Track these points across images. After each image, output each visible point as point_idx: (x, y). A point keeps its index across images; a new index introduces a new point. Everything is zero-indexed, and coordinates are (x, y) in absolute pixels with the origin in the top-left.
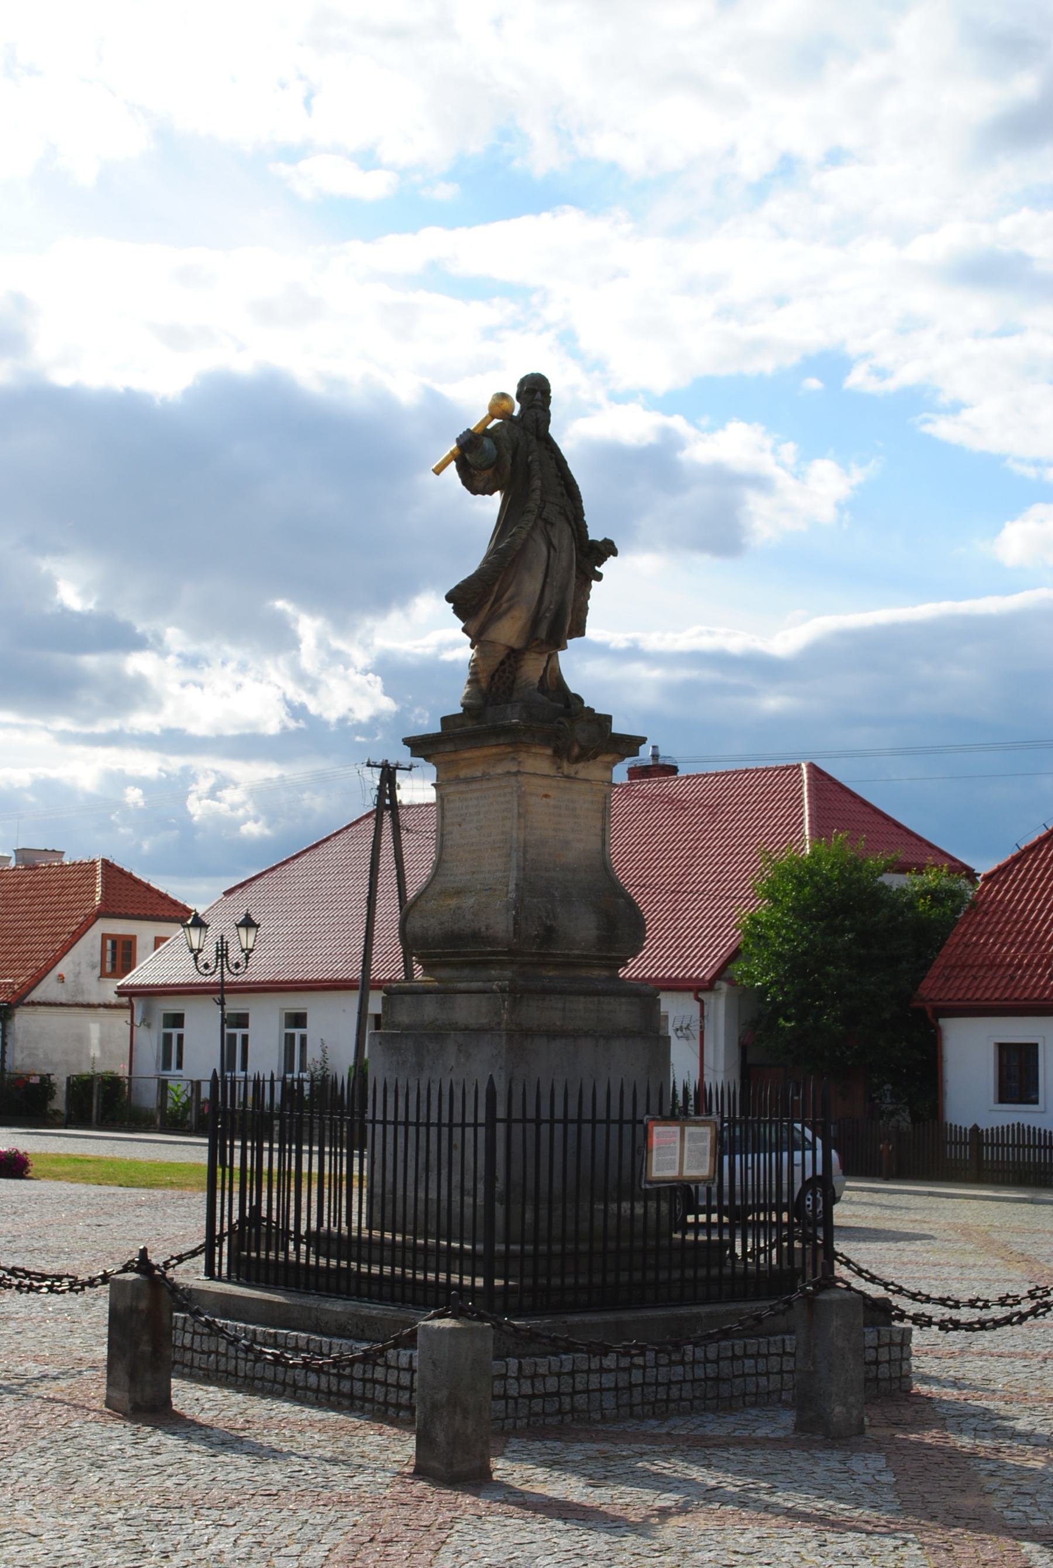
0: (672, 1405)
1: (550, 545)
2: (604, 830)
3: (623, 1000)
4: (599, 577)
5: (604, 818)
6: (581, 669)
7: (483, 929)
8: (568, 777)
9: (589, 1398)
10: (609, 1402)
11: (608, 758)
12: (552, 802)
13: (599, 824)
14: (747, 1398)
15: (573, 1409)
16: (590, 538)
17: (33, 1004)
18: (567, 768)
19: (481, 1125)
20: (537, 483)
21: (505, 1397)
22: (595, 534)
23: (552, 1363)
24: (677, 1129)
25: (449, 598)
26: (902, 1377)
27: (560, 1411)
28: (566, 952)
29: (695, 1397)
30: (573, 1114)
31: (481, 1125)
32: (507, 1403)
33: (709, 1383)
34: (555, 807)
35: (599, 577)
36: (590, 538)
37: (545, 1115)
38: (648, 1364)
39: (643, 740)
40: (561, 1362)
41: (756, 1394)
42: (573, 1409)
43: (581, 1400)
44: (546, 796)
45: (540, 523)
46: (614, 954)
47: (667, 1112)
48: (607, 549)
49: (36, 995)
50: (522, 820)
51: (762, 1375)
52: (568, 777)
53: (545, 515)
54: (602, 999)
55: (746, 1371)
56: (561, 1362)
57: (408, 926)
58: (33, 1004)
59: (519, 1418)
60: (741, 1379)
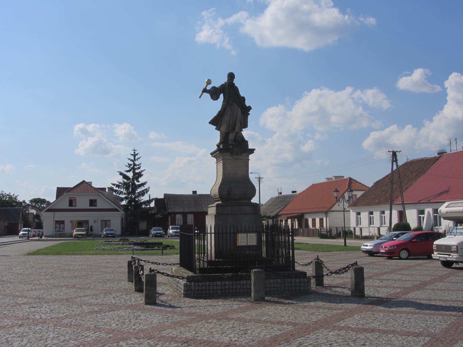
4: (249, 114)
8: (236, 159)
11: (246, 154)
17: (332, 211)
18: (235, 157)
21: (191, 290)
24: (245, 235)
35: (249, 114)
39: (255, 149)
42: (209, 293)
43: (212, 292)
49: (333, 209)
52: (236, 159)
58: (332, 211)
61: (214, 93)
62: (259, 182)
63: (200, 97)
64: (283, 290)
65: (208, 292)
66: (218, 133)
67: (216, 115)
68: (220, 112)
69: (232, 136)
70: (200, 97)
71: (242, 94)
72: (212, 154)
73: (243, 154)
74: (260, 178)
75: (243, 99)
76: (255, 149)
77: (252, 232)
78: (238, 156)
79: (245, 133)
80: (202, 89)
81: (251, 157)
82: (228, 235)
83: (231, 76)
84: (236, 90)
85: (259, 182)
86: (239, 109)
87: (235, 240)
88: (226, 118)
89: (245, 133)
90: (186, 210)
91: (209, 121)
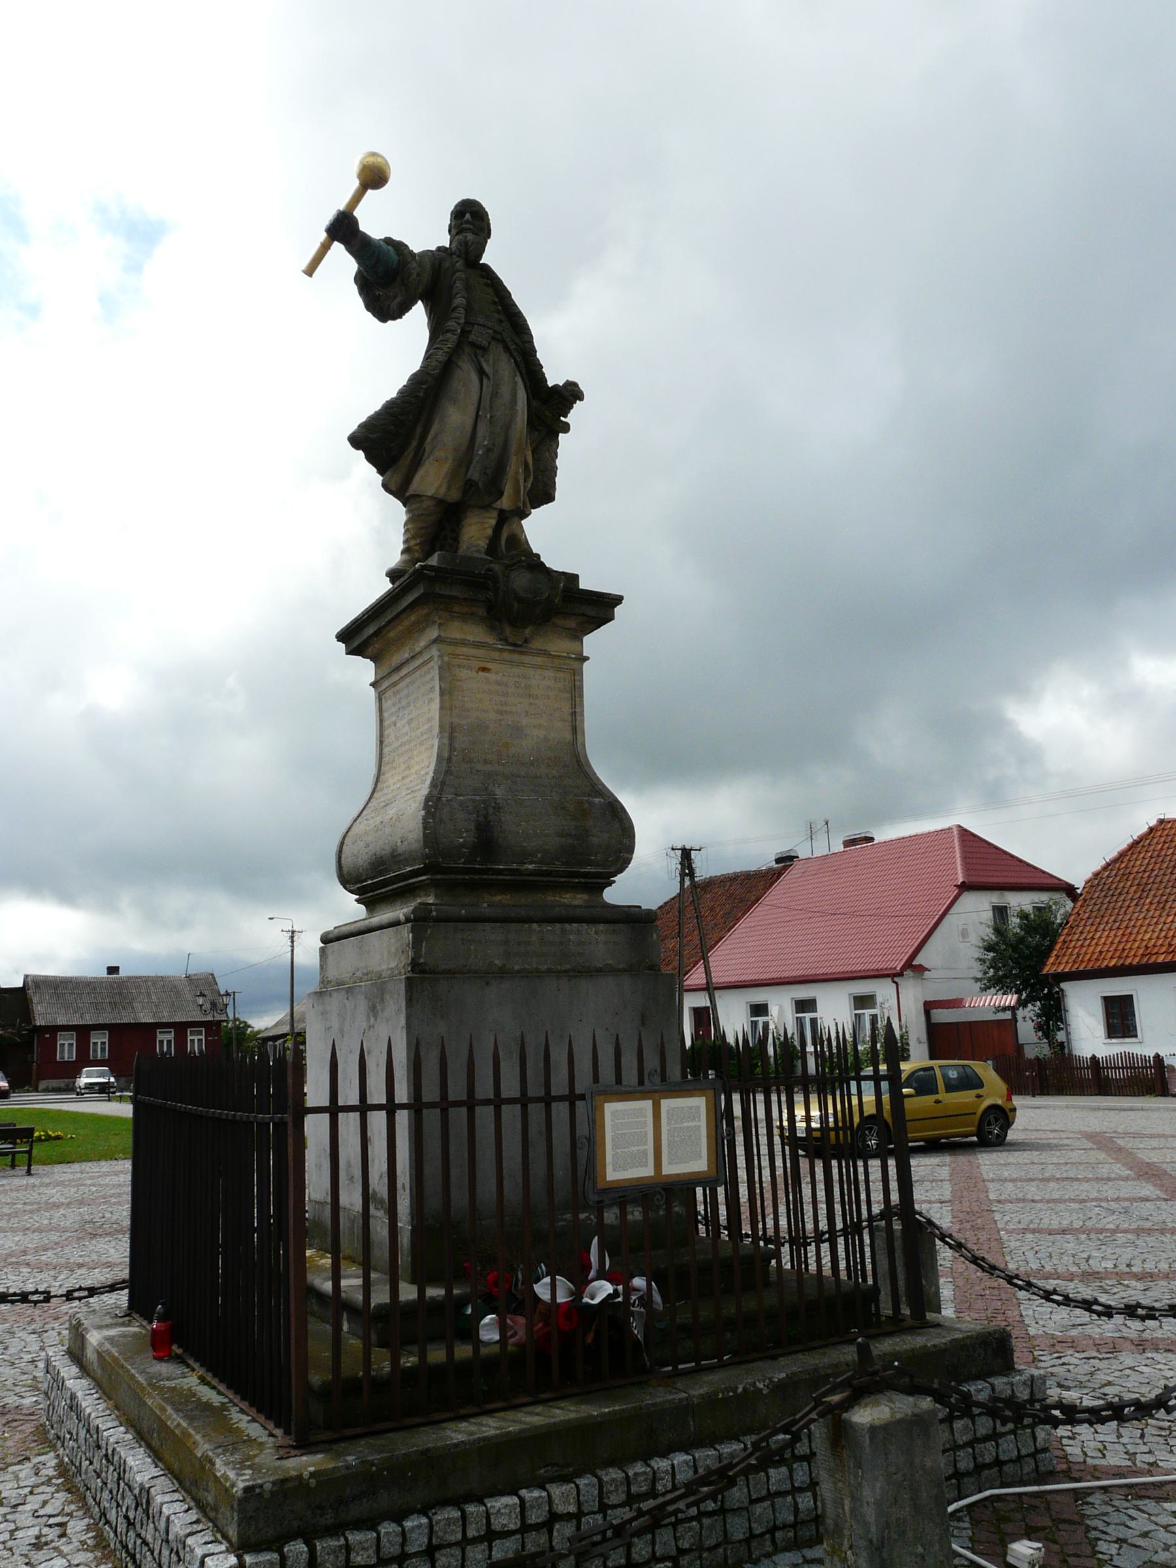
1: (482, 373)
2: (574, 714)
3: (602, 927)
4: (566, 428)
5: (573, 699)
6: (547, 533)
7: (399, 844)
11: (572, 623)
12: (492, 677)
13: (567, 709)
14: (779, 1535)
16: (550, 384)
19: (402, 1106)
20: (459, 301)
22: (554, 377)
23: (384, 1540)
24: (647, 1105)
25: (356, 441)
26: (1038, 1451)
28: (515, 866)
29: (682, 1552)
30: (457, 1091)
31: (402, 1106)
33: (706, 1521)
34: (498, 683)
35: (566, 428)
36: (550, 384)
37: (485, 1089)
38: (585, 1509)
39: (618, 600)
40: (403, 1534)
41: (794, 1526)
44: (484, 669)
45: (468, 349)
46: (589, 869)
47: (630, 1076)
48: (570, 394)
50: (446, 697)
51: (801, 1490)
53: (472, 338)
54: (567, 926)
55: (773, 1488)
56: (403, 1534)
57: (343, 856)
60: (767, 1504)
61: (388, 278)
62: (292, 942)
63: (310, 271)
66: (397, 511)
67: (392, 393)
68: (416, 380)
69: (475, 532)
70: (310, 271)
72: (345, 636)
74: (293, 932)
76: (618, 600)
80: (327, 217)
81: (592, 642)
85: (292, 942)
87: (586, 1147)
88: (455, 419)
90: (88, 1019)
91: (353, 427)
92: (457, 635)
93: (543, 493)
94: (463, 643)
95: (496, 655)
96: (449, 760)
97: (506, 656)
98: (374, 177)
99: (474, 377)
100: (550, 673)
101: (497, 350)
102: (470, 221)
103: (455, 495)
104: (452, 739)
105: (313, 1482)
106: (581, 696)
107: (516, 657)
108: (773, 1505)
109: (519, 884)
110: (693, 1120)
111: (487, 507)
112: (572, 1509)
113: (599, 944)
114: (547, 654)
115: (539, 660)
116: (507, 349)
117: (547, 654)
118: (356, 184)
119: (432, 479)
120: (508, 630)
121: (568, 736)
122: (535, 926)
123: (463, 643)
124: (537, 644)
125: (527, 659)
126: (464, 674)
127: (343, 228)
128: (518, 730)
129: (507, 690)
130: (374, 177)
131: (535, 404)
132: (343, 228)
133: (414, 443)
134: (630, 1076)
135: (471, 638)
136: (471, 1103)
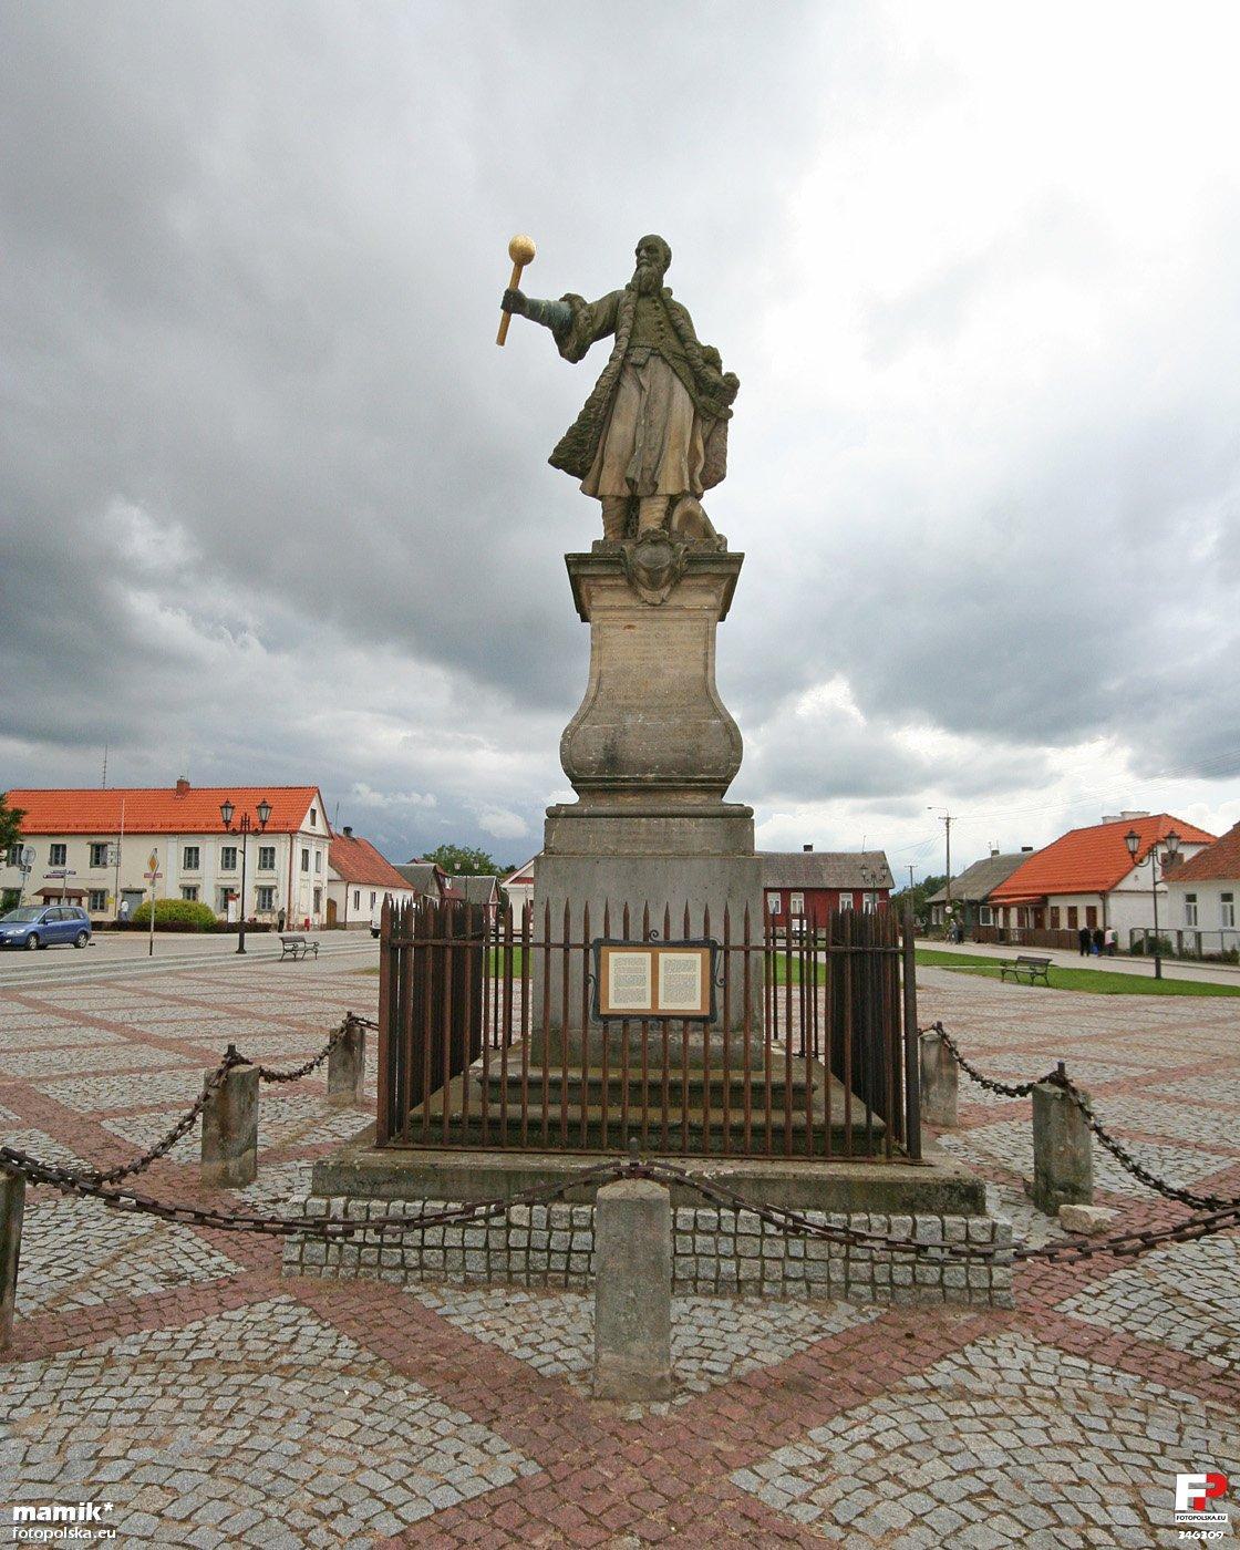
0: (572, 1279)
1: (641, 388)
9: (445, 1256)
10: (476, 1263)
12: (637, 632)
13: (701, 651)
15: (422, 1266)
24: (647, 956)
27: (402, 1265)
32: (327, 1249)
39: (742, 555)
42: (422, 1266)
44: (629, 627)
45: (630, 369)
46: (702, 776)
50: (596, 652)
53: (633, 359)
55: (698, 1251)
59: (344, 1266)
61: (572, 328)
63: (501, 341)
64: (837, 1276)
65: (412, 1257)
66: (596, 506)
70: (501, 341)
71: (705, 336)
73: (685, 582)
75: (712, 358)
77: (687, 944)
78: (665, 592)
79: (713, 503)
82: (557, 954)
83: (653, 254)
84: (676, 322)
86: (678, 385)
87: (594, 982)
89: (713, 503)
90: (789, 884)
92: (607, 603)
93: (713, 474)
94: (611, 608)
95: (639, 615)
96: (595, 699)
97: (648, 614)
98: (522, 257)
99: (635, 392)
100: (688, 624)
101: (656, 365)
102: (653, 254)
103: (626, 492)
104: (599, 683)
105: (358, 1167)
106: (714, 640)
107: (657, 614)
108: (697, 1261)
109: (644, 790)
110: (689, 969)
111: (653, 495)
112: (525, 1223)
113: (697, 834)
114: (681, 608)
115: (677, 615)
116: (665, 360)
117: (681, 608)
118: (512, 264)
119: (610, 482)
120: (646, 594)
121: (701, 671)
122: (643, 820)
123: (611, 608)
124: (674, 601)
125: (666, 615)
126: (611, 632)
127: (514, 302)
128: (657, 672)
129: (646, 641)
130: (522, 257)
131: (703, 399)
132: (514, 302)
133: (598, 456)
134: (636, 934)
135: (617, 604)
136: (566, 946)
